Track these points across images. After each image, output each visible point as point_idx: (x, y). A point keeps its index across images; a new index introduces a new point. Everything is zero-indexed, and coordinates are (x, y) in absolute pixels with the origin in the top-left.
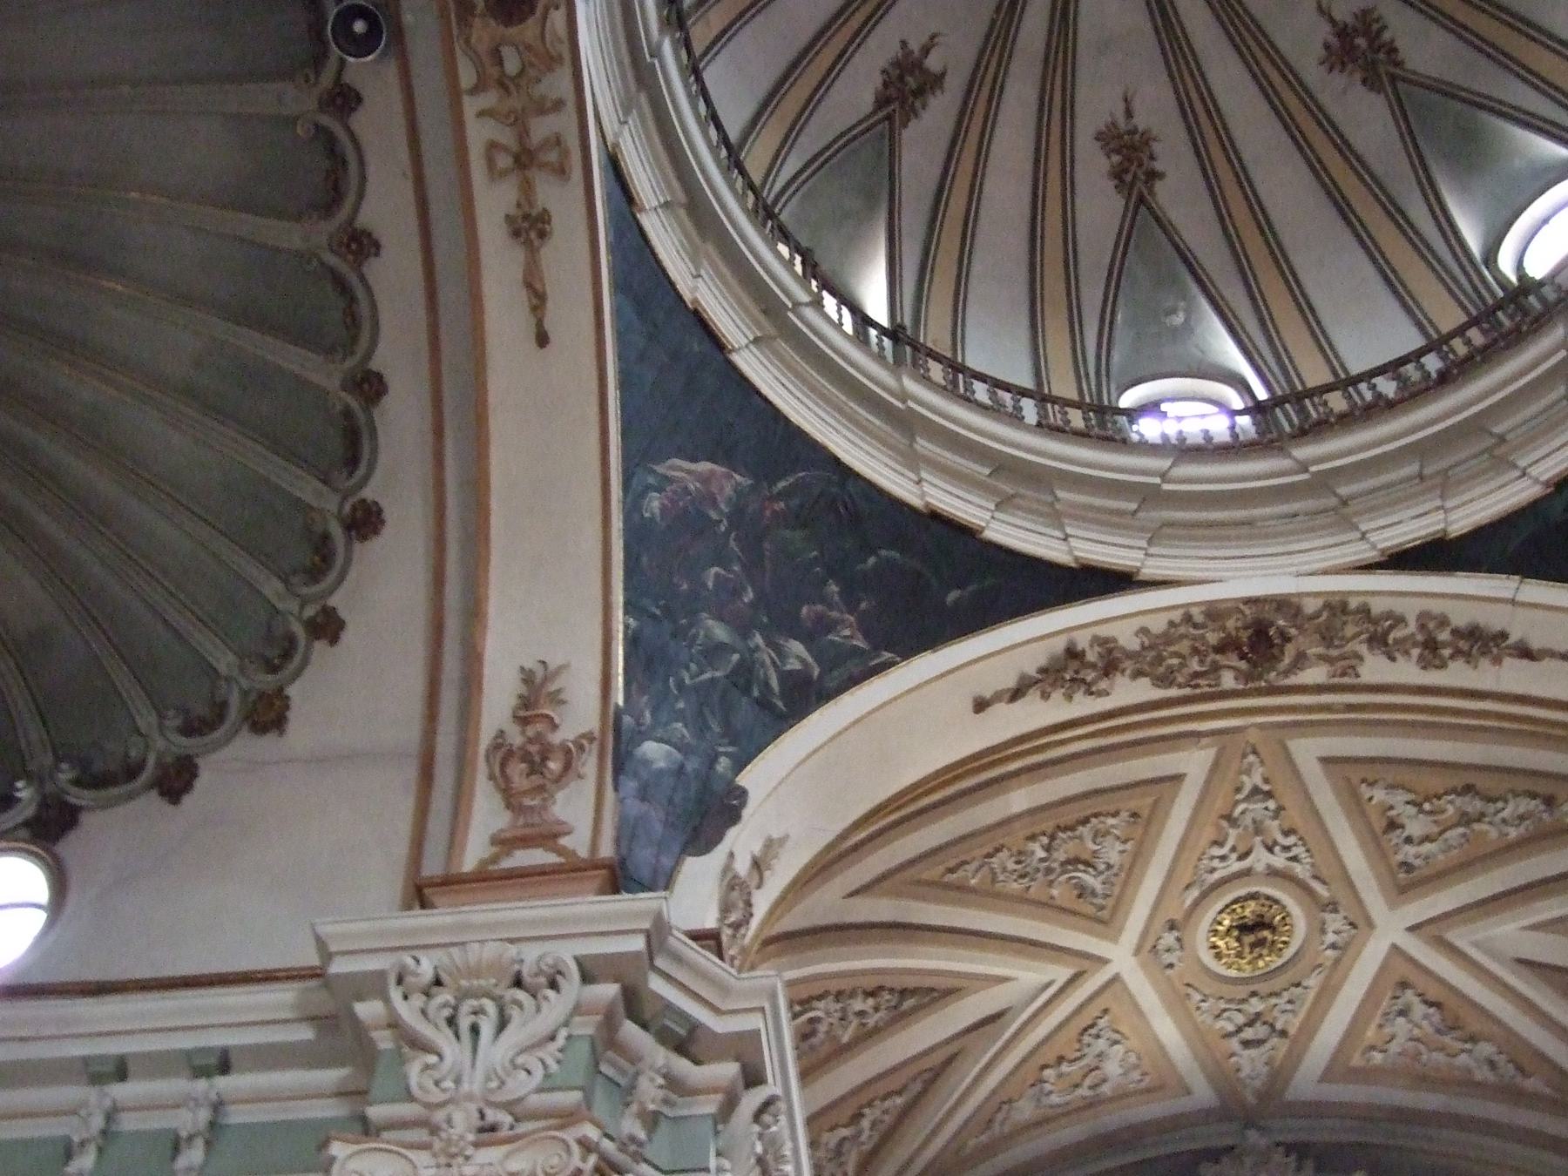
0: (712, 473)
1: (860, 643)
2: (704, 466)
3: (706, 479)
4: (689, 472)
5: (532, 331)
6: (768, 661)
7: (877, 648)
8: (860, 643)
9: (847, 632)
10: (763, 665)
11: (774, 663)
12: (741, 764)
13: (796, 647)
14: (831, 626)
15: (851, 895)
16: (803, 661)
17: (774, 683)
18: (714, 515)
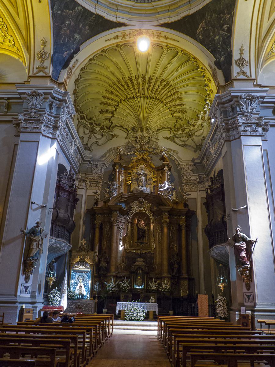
0: (201, 25)
1: (229, 16)
2: (200, 26)
3: (202, 27)
4: (200, 29)
5: (177, 42)
6: (223, 32)
7: (231, 14)
8: (229, 16)
9: (227, 17)
10: (224, 33)
11: (225, 32)
12: (230, 47)
13: (225, 26)
14: (225, 19)
15: (268, 21)
16: (226, 27)
17: (226, 33)
18: (205, 28)
